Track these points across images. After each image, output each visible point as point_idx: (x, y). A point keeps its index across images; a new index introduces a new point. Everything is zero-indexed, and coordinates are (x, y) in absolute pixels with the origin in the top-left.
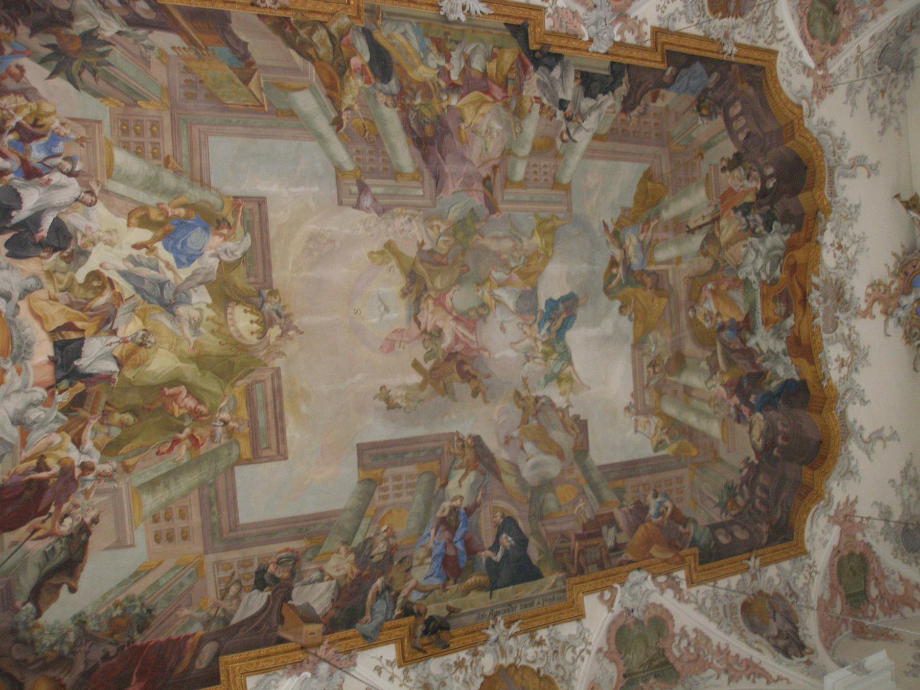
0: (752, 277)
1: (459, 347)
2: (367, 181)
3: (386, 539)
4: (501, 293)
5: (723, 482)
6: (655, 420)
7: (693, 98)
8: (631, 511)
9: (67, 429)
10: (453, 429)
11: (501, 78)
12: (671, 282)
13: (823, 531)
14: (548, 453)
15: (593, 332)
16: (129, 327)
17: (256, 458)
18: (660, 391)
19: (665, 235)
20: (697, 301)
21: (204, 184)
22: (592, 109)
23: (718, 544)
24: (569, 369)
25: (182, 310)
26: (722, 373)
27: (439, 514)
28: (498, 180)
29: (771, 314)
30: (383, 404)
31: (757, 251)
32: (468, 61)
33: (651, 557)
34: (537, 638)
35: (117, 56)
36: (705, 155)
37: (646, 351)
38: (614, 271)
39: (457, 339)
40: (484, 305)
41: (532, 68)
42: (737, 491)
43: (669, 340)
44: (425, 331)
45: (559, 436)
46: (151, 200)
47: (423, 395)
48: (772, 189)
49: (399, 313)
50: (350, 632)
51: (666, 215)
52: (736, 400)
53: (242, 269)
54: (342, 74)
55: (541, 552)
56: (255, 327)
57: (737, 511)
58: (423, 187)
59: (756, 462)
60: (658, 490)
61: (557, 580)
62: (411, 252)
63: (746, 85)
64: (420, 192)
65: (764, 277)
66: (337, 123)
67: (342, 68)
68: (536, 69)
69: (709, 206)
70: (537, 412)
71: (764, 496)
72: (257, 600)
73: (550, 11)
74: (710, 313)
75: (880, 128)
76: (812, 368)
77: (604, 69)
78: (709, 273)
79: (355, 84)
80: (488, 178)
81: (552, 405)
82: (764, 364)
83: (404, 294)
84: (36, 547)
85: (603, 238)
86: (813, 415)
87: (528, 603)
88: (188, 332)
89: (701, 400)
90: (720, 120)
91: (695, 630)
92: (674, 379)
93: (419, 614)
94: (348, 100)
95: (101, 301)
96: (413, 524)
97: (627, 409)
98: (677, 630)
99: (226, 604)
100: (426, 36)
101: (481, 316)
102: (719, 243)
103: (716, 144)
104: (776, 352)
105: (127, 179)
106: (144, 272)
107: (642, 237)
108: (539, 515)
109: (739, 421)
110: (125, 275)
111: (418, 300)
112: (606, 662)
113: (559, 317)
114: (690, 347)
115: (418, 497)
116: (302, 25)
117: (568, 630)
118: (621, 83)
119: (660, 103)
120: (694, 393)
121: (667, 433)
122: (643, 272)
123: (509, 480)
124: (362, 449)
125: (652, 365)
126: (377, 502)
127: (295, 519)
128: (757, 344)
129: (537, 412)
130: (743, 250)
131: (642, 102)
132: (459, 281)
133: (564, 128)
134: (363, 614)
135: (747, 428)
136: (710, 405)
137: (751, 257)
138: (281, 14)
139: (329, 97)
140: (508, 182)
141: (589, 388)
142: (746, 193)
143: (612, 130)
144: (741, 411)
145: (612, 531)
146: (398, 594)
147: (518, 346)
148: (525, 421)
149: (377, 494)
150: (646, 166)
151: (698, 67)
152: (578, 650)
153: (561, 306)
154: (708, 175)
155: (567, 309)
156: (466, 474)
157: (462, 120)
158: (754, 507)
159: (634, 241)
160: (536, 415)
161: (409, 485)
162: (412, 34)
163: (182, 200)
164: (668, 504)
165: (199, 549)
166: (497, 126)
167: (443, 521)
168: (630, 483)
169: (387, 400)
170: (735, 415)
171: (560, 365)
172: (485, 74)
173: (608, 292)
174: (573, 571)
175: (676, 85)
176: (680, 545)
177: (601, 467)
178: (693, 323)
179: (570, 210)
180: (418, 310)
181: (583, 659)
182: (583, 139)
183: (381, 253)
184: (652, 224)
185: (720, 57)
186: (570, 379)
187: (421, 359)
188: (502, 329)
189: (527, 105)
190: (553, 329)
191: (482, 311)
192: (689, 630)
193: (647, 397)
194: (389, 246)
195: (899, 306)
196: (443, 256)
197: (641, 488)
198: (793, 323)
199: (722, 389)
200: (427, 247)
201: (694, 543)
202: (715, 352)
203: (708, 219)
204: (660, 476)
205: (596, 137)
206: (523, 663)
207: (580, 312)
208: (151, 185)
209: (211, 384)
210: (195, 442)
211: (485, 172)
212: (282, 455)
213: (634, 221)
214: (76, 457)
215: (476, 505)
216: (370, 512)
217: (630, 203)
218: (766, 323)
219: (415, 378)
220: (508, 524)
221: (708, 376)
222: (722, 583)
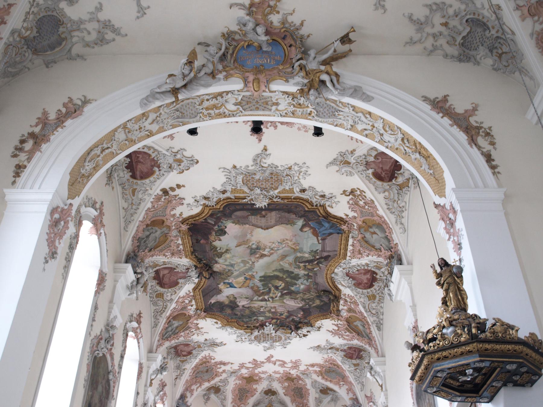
75: (415, 18)
195: (257, 25)
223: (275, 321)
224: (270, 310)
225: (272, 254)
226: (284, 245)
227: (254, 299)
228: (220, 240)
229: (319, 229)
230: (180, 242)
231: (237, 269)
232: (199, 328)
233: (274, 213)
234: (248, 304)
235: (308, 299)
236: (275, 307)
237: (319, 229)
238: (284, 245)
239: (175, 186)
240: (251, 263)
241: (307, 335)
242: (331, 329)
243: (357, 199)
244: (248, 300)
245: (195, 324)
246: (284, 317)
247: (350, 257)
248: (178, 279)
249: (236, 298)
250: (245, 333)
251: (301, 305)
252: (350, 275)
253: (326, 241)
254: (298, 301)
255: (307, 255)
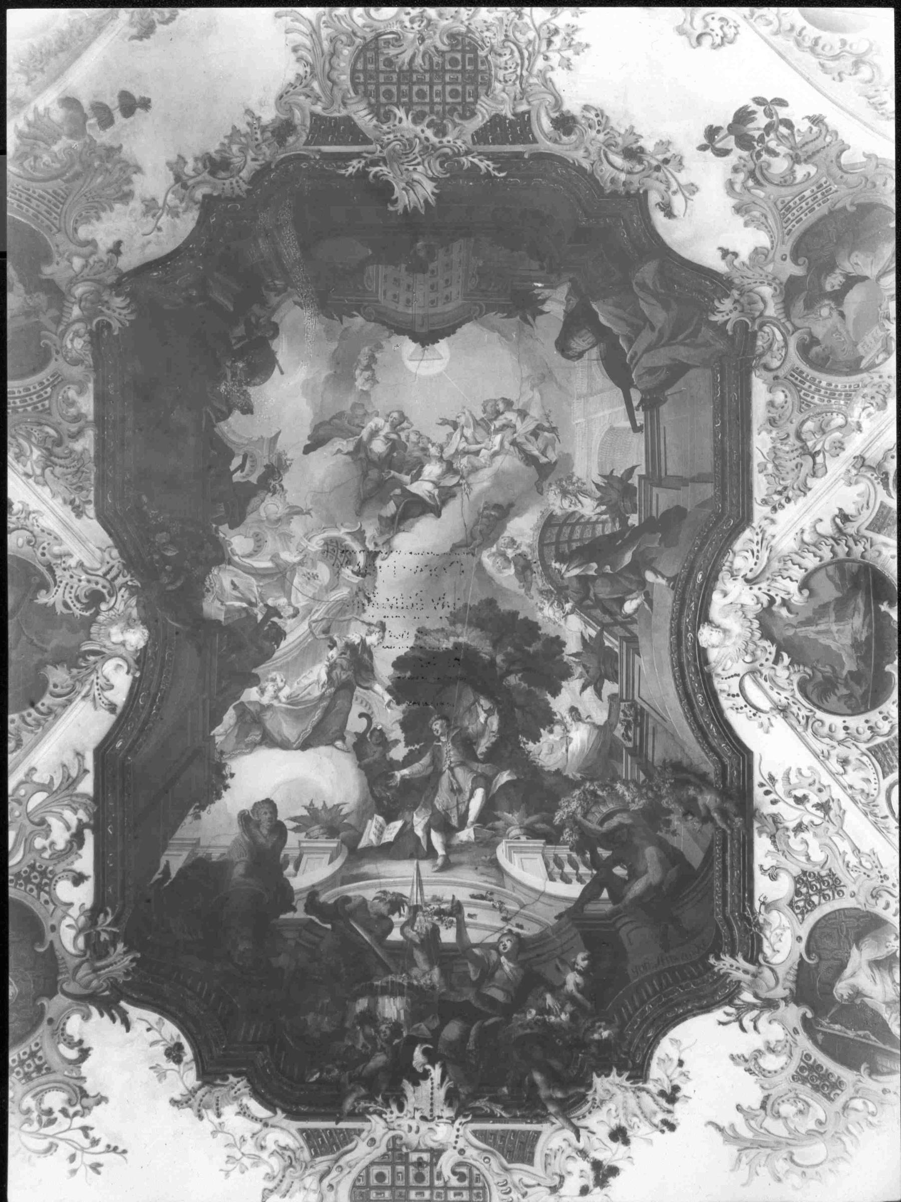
223: (452, 1031)
224: (435, 931)
225: (447, 495)
226: (498, 438)
227: (363, 844)
228: (248, 410)
229: (630, 341)
230: (87, 405)
231: (300, 602)
232: (84, 1094)
233: (458, 251)
234: (330, 882)
235: (609, 839)
236: (457, 908)
237: (630, 341)
238: (498, 438)
239: (112, 102)
240: (361, 558)
241: (614, 1171)
242: (730, 1117)
243: (759, 155)
244: (333, 844)
245: (71, 1043)
246: (498, 995)
247: (765, 502)
248: (42, 664)
249: (279, 830)
250: (306, 1155)
251: (574, 890)
252: (775, 631)
253: (664, 409)
254: (564, 852)
255: (588, 508)
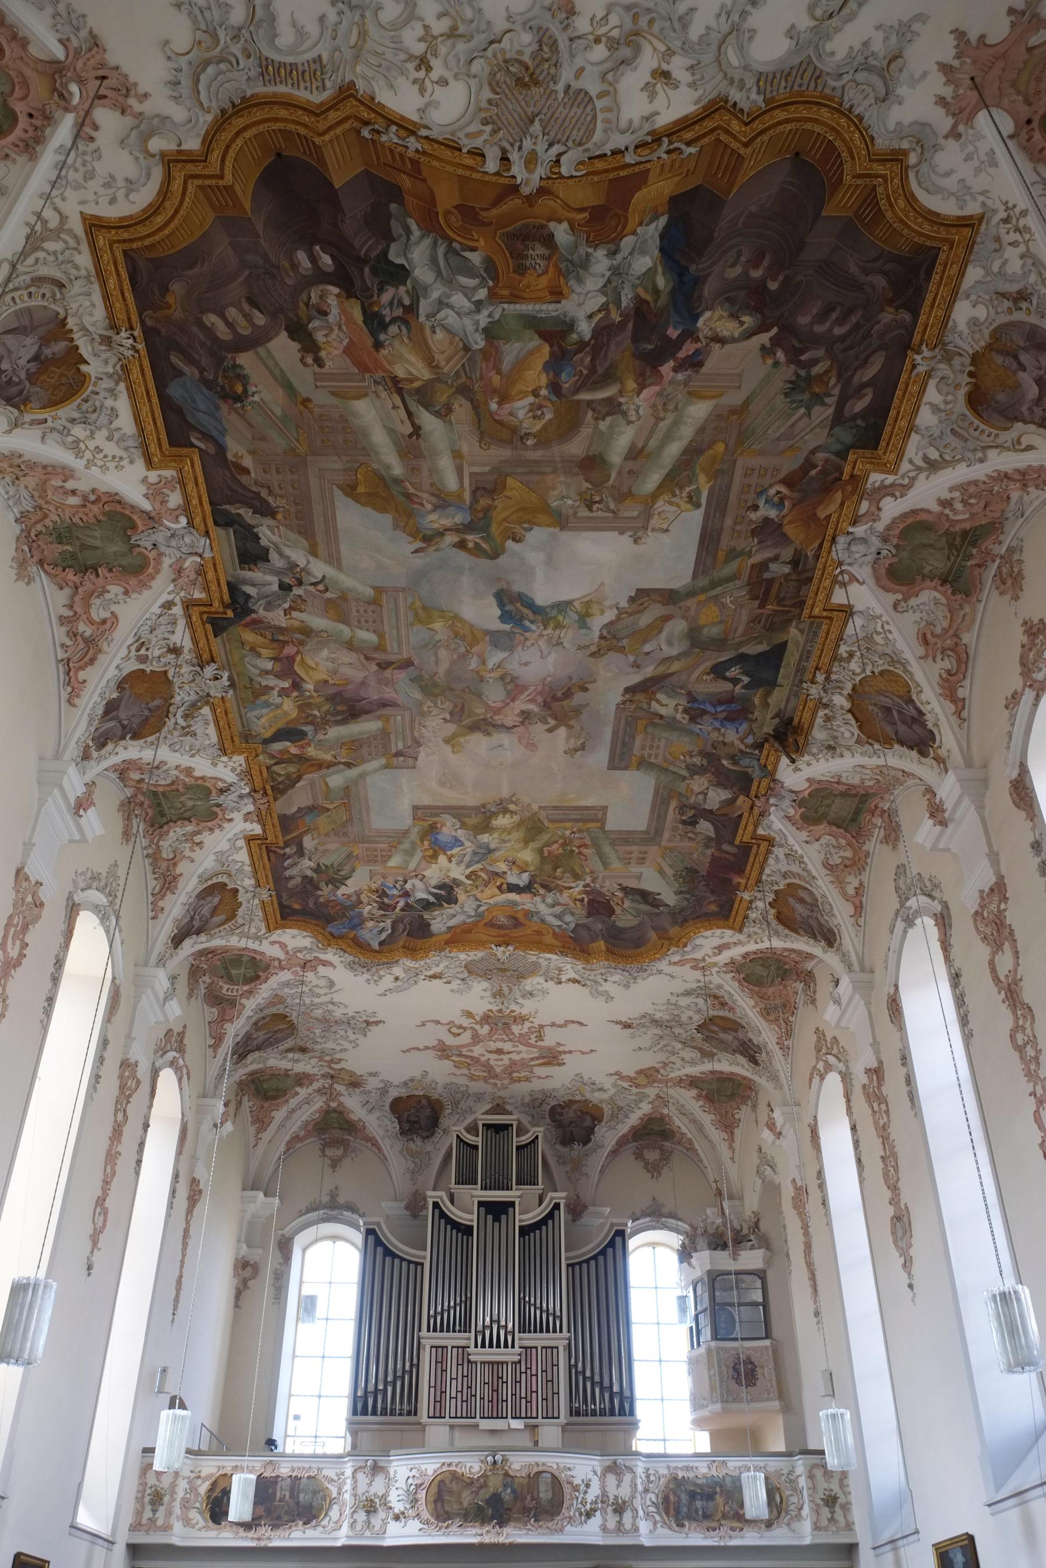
0: (483, 319)
1: (540, 699)
2: (394, 751)
3: (691, 756)
4: (491, 663)
5: (780, 401)
6: (660, 505)
7: (224, 408)
8: (760, 542)
9: (561, 892)
10: (613, 708)
11: (275, 645)
12: (487, 469)
13: (968, 158)
14: (661, 631)
15: (540, 574)
16: (502, 867)
17: (603, 821)
18: (624, 496)
19: (425, 473)
20: (514, 430)
21: (406, 833)
22: (281, 554)
23: (864, 414)
24: (576, 604)
25: (492, 846)
26: (621, 393)
27: (685, 722)
28: (381, 657)
29: (544, 282)
30: (579, 753)
31: (441, 304)
32: (267, 672)
33: (829, 517)
34: (845, 655)
35: (326, 861)
36: (305, 395)
37: (571, 512)
38: (471, 545)
39: (532, 701)
40: (502, 678)
41: (254, 615)
42: (802, 373)
43: (562, 479)
44: (522, 723)
45: (645, 620)
46: (418, 855)
47: (577, 727)
48: (332, 257)
49: (504, 739)
50: (755, 783)
51: (398, 470)
52: (666, 369)
53: (466, 820)
54: (307, 760)
55: (761, 643)
56: (508, 816)
57: (834, 373)
58: (395, 716)
59: (775, 330)
60: (750, 504)
61: (797, 627)
62: (452, 728)
63: (170, 299)
64: (399, 718)
65: (482, 294)
66: (349, 765)
67: (301, 759)
68: (254, 611)
69: (378, 396)
70: (615, 637)
71: (834, 316)
72: (705, 827)
73: (182, 594)
74: (533, 408)
76: (652, 177)
77: (228, 534)
78: (475, 408)
79: (311, 751)
80: (379, 664)
81: (612, 623)
82: (624, 304)
83: (489, 734)
84: (627, 904)
85: (432, 556)
86: (741, 179)
87: (806, 655)
88: (508, 844)
89: (650, 437)
90: (245, 359)
91: (951, 490)
92: (613, 475)
93: (766, 740)
94: (328, 757)
95: (484, 876)
96: (687, 739)
97: (636, 541)
98: (936, 508)
99: (699, 839)
100: (254, 703)
101: (512, 681)
102: (430, 381)
103: (281, 370)
104: (608, 274)
105: (407, 863)
106: (467, 859)
107: (429, 507)
108: (720, 643)
109: (701, 364)
110: (468, 867)
111: (494, 726)
112: (913, 602)
113: (519, 611)
114: (576, 447)
115: (664, 735)
116: (274, 780)
117: (856, 626)
118: (239, 515)
119: (247, 462)
120: (640, 445)
121: (681, 489)
122: (472, 508)
123: (676, 666)
124: (612, 765)
125: (589, 505)
126: (659, 761)
127: (654, 805)
128: (590, 317)
129: (615, 637)
130: (440, 335)
131: (254, 489)
132: (479, 695)
133: (311, 588)
134: (746, 773)
135: (717, 346)
136: (663, 419)
137: (449, 317)
138: (269, 792)
139: (328, 768)
140: (380, 648)
141: (602, 584)
142: (350, 320)
143: (300, 533)
144: (687, 357)
145: (773, 566)
146: (741, 751)
147: (546, 652)
148: (622, 650)
149: (652, 760)
150: (338, 493)
151: (175, 391)
152: (879, 629)
153: (507, 608)
154: (334, 394)
155: (511, 602)
156: (658, 701)
157: (326, 682)
158: (841, 339)
159: (433, 517)
160: (619, 640)
161: (653, 740)
162: (257, 712)
163: (418, 842)
164: (772, 492)
165: (655, 848)
166: (325, 653)
167: (693, 719)
168: (725, 543)
169: (576, 750)
170: (689, 372)
171: (571, 614)
172: (275, 659)
173: (495, 555)
174: (796, 611)
175: (215, 434)
176: (837, 475)
177: (695, 576)
178: (544, 440)
179: (403, 590)
180: (503, 726)
181: (890, 632)
182: (319, 569)
183: (453, 746)
184: (412, 490)
185: (144, 352)
186: (588, 604)
187: (547, 727)
188: (526, 664)
189: (296, 624)
190: (531, 617)
191: (508, 680)
192: (946, 495)
193: (627, 514)
194: (447, 741)
196: (455, 706)
197: (738, 528)
198: (565, 225)
199: (645, 393)
200: (448, 717)
201: (843, 455)
202: (589, 403)
203: (398, 401)
204: (733, 499)
205: (313, 552)
206: (858, 679)
207: (516, 588)
208: (410, 853)
209: (545, 838)
210: (585, 846)
211: (374, 668)
212: (604, 809)
213: (410, 515)
214: (581, 888)
215: (689, 694)
216: (665, 765)
217: (387, 519)
218: (557, 294)
219: (562, 731)
220: (718, 671)
221: (620, 418)
222: (926, 418)
